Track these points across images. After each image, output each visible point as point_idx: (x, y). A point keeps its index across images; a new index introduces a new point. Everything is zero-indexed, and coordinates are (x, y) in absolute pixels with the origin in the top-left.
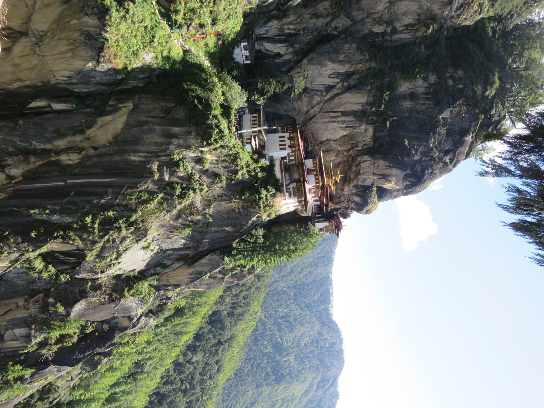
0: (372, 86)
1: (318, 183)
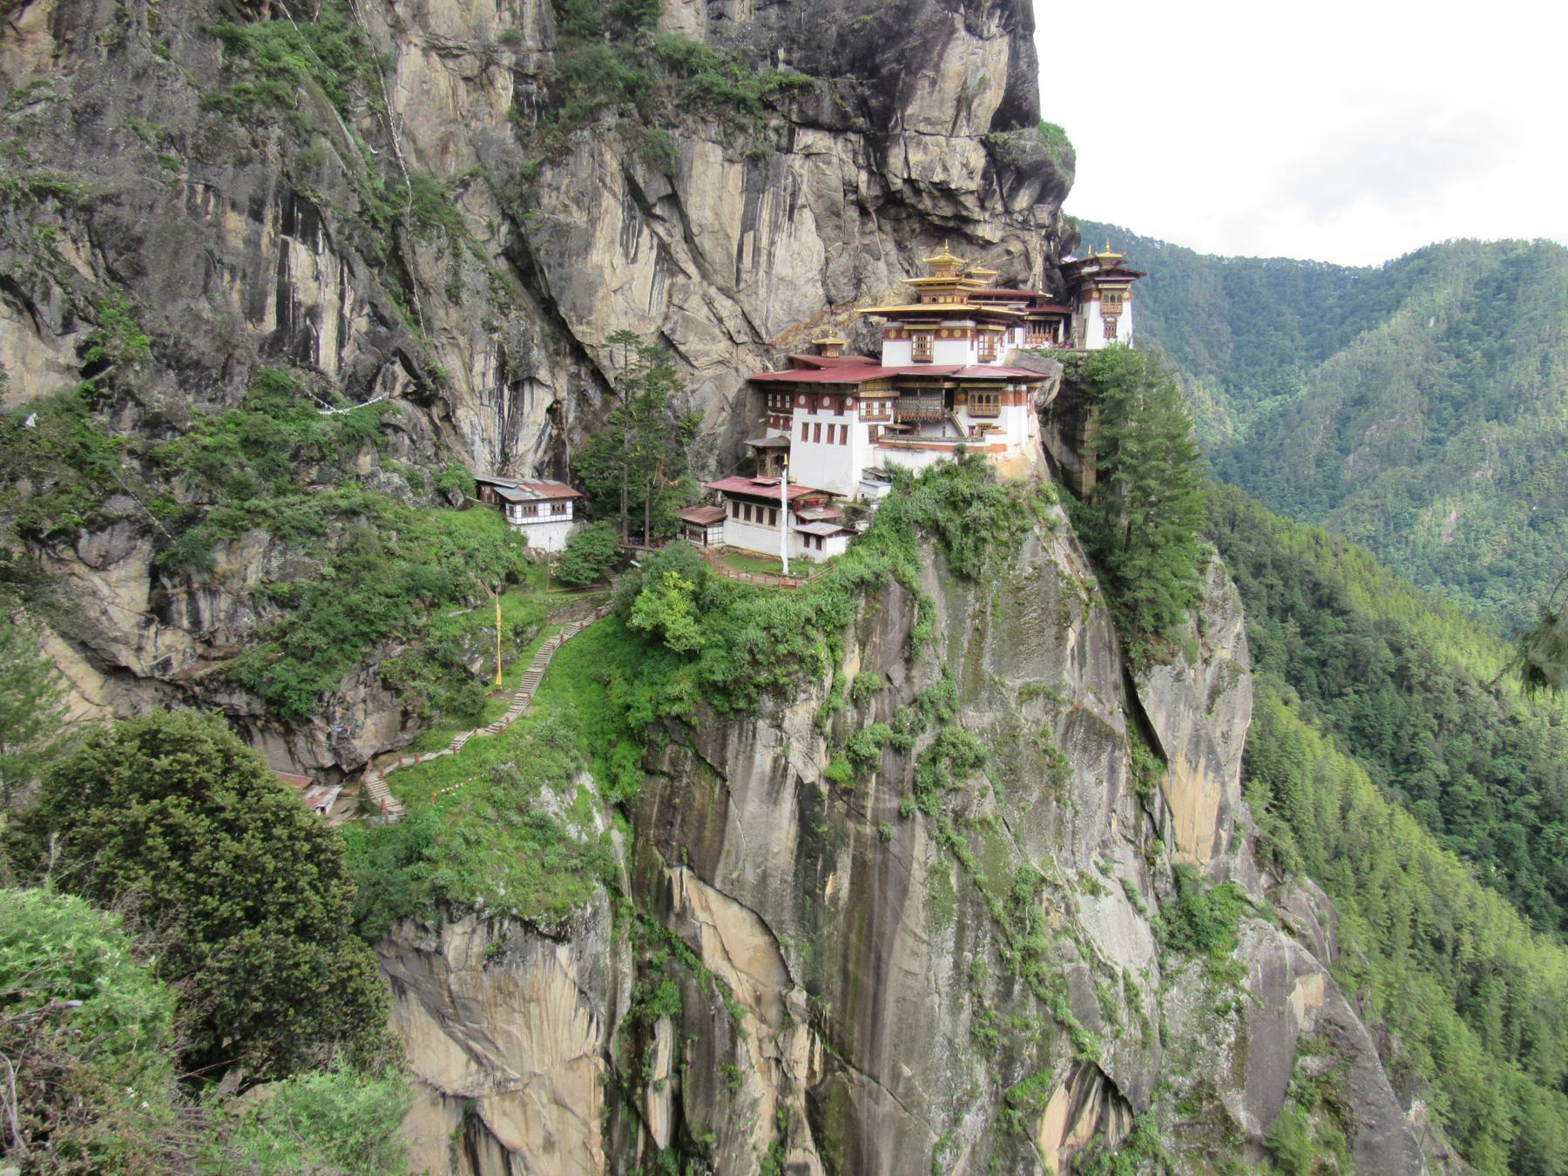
0: (675, 127)
1: (964, 331)
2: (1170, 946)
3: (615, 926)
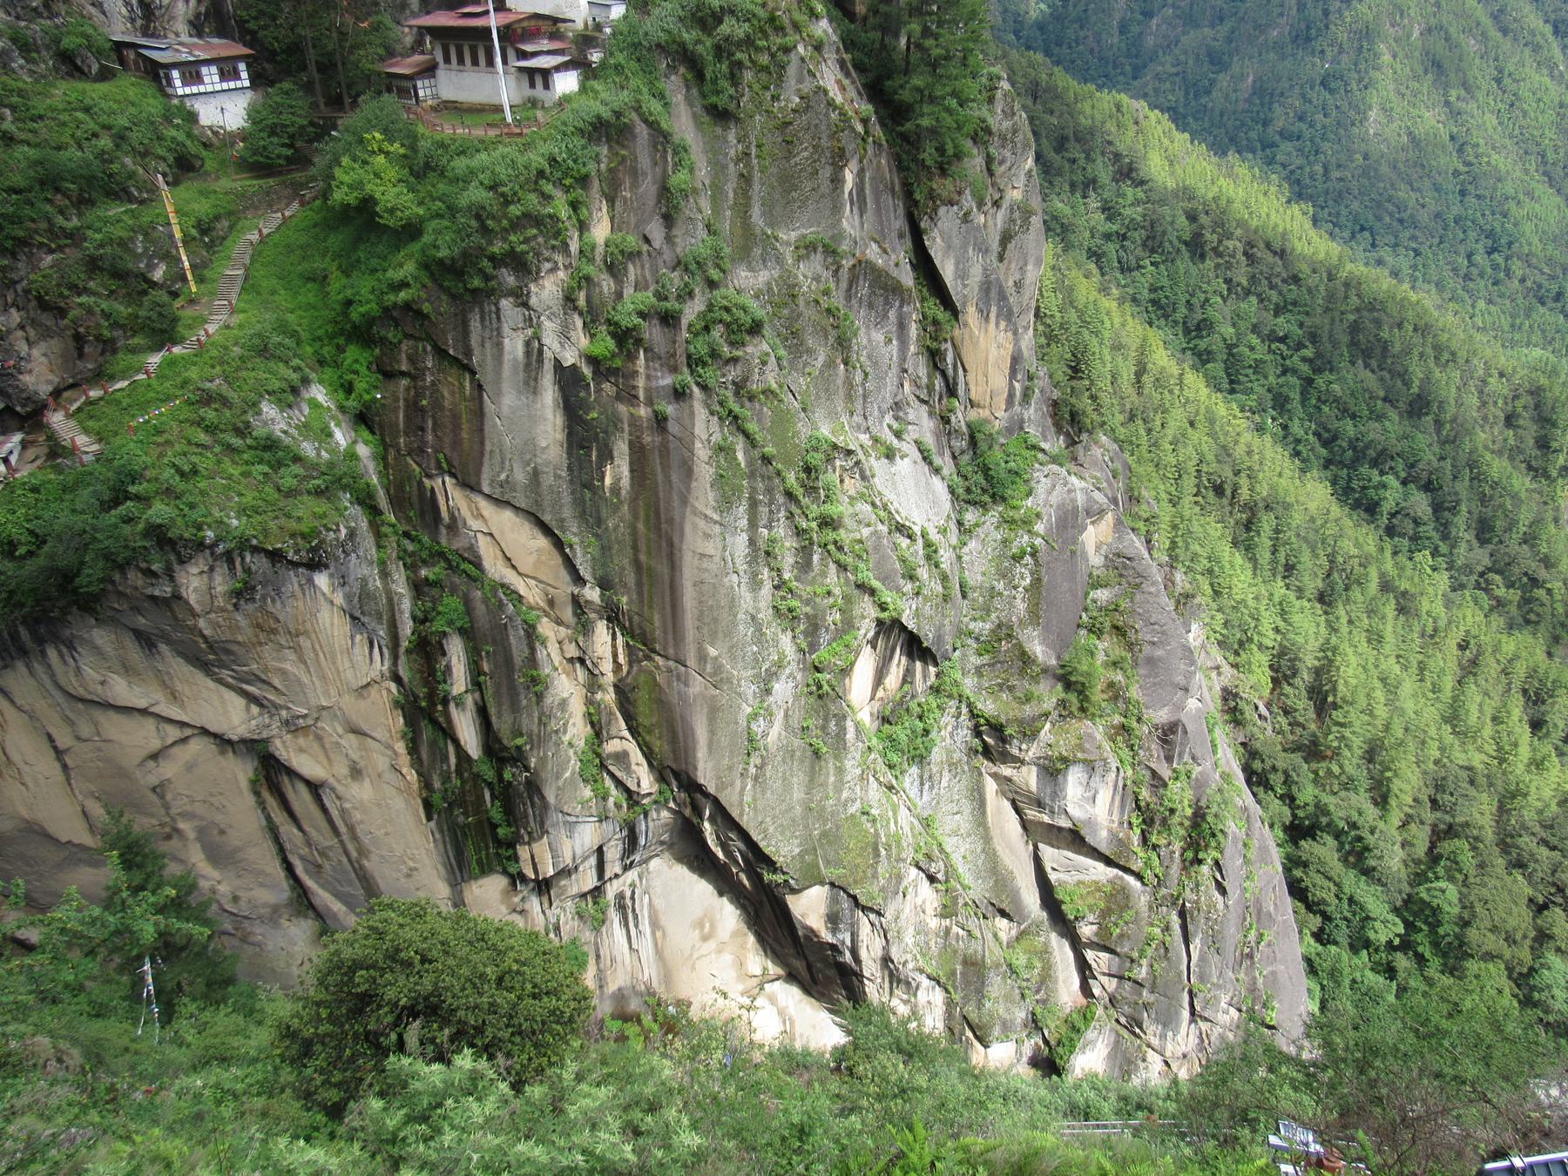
2: (968, 502)
3: (379, 547)
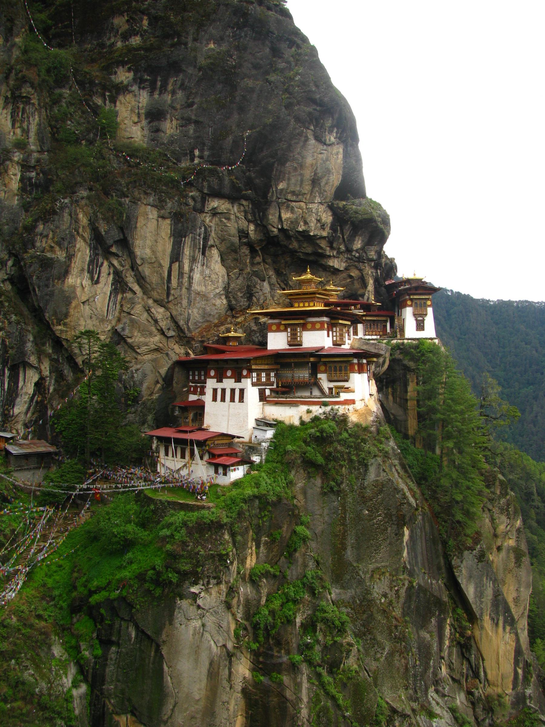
1: (322, 323)
